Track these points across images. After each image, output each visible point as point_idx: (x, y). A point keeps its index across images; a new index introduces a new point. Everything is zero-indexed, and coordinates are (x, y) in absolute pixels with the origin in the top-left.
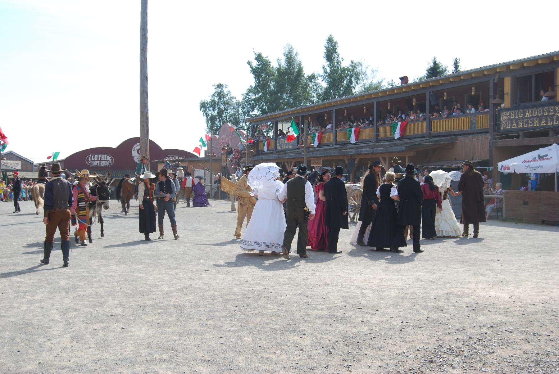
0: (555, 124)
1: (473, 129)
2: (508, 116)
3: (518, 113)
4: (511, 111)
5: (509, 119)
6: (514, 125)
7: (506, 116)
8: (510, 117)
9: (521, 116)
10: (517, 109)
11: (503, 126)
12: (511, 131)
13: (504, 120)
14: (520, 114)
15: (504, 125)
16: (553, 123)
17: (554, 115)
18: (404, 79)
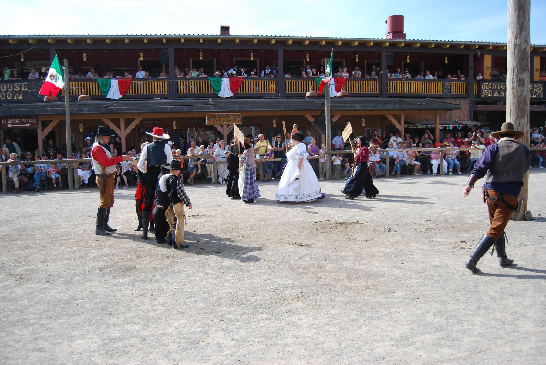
0: (533, 96)
1: (447, 94)
2: (490, 86)
3: (500, 85)
4: (493, 83)
5: (490, 89)
6: (495, 94)
7: (488, 86)
8: (492, 87)
9: (503, 87)
10: (499, 82)
11: (485, 94)
12: (492, 98)
13: (485, 89)
14: (502, 86)
15: (486, 93)
16: (532, 95)
17: (533, 90)
18: (225, 29)
